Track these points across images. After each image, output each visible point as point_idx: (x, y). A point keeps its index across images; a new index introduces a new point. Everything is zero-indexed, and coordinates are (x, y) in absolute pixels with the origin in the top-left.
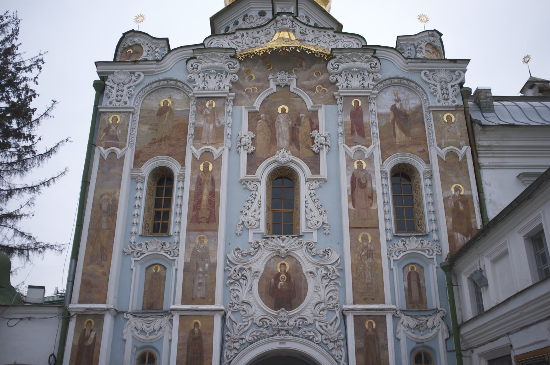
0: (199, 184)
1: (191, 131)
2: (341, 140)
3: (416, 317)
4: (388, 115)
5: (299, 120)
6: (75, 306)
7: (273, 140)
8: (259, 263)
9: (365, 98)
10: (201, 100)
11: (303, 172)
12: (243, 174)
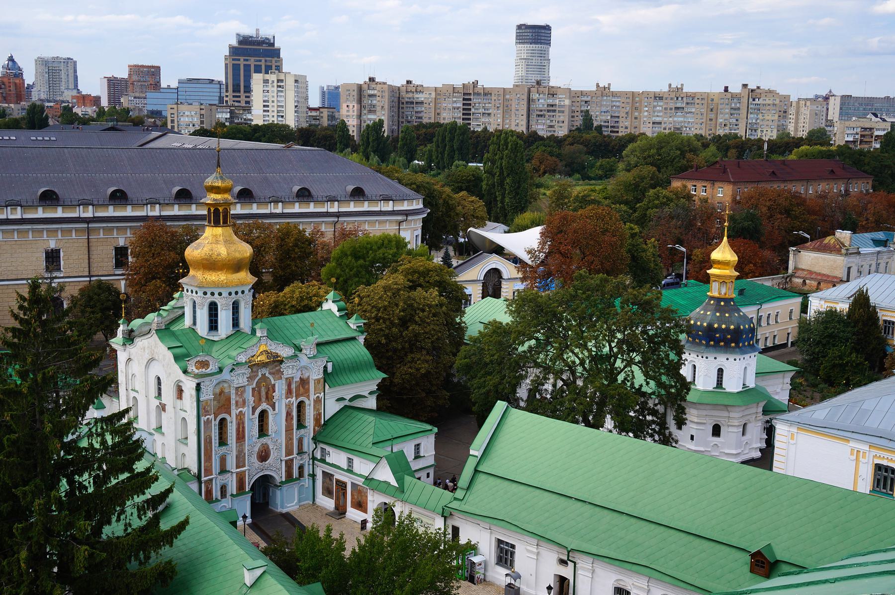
0: (238, 425)
1: (233, 402)
2: (284, 397)
6: (203, 479)
7: (260, 399)
8: (256, 449)
10: (237, 388)
11: (270, 412)
12: (251, 417)
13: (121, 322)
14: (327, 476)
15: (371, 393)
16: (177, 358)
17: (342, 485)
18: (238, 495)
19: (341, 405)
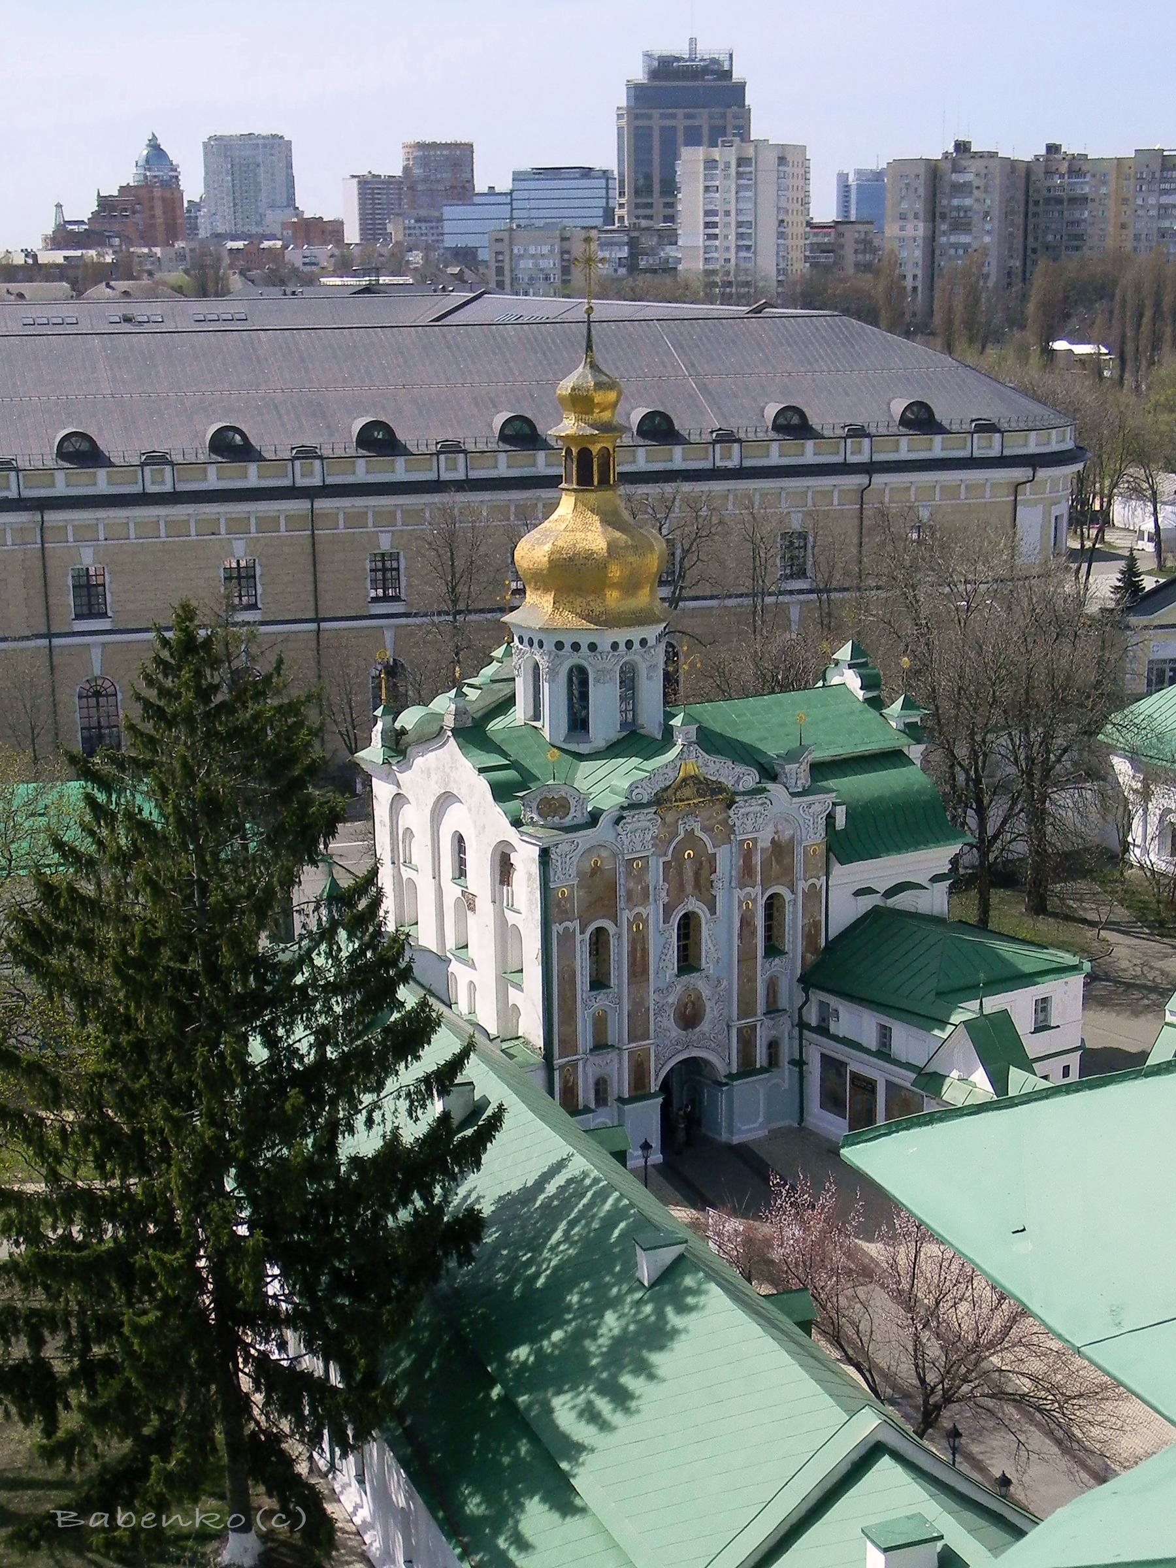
0: (633, 942)
1: (621, 892)
3: (772, 1019)
4: (767, 849)
5: (701, 863)
6: (557, 1062)
7: (681, 887)
8: (672, 999)
9: (755, 840)
13: (379, 712)
14: (832, 1065)
15: (936, 879)
16: (501, 793)
17: (865, 1086)
18: (632, 1100)
19: (866, 903)
